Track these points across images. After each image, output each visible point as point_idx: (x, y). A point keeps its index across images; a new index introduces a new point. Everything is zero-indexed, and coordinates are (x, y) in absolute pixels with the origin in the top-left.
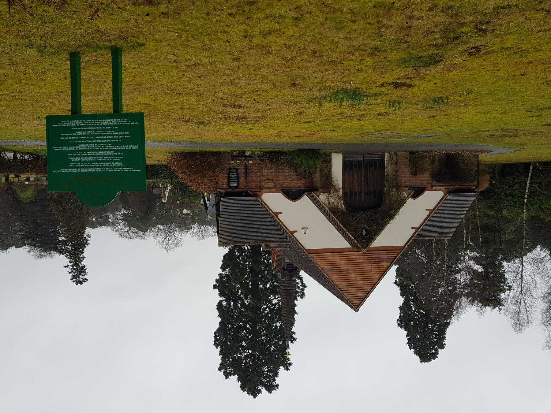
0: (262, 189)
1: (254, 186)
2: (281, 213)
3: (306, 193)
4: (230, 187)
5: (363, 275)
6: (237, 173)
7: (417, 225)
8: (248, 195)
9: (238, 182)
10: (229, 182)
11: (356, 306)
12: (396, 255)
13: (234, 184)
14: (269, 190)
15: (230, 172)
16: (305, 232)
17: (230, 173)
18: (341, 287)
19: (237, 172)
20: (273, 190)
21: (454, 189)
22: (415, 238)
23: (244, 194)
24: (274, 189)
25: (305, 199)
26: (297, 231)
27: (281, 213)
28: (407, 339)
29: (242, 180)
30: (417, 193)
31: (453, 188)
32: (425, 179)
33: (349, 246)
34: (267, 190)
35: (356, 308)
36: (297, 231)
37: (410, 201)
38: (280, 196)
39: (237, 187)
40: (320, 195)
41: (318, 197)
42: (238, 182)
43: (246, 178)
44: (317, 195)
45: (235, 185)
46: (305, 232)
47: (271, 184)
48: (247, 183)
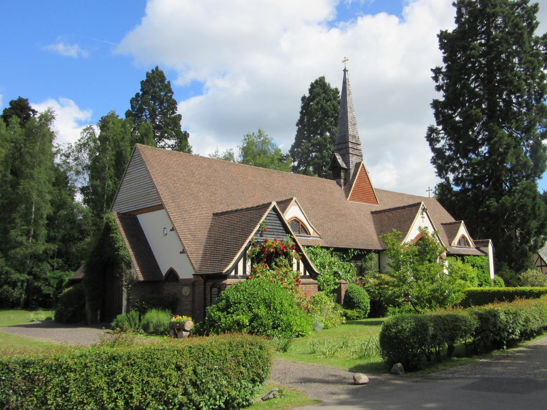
0: (192, 284)
1: (199, 288)
3: (163, 279)
8: (202, 276)
42: (211, 294)
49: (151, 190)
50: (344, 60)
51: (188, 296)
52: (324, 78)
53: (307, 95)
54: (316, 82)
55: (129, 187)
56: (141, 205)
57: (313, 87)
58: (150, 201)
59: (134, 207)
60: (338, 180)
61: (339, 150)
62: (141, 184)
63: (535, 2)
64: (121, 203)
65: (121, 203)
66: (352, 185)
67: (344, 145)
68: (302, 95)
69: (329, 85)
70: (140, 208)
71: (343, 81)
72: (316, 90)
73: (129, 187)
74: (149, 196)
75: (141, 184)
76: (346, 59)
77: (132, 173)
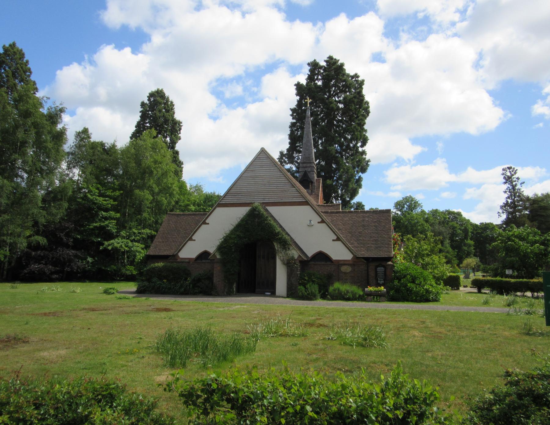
2: (333, 240)
4: (384, 266)
6: (377, 280)
7: (204, 226)
9: (376, 272)
10: (385, 271)
11: (263, 152)
12: (224, 198)
13: (380, 269)
14: (345, 262)
15: (384, 281)
17: (384, 280)
18: (276, 170)
19: (377, 281)
20: (342, 262)
23: (371, 260)
24: (340, 264)
25: (310, 254)
26: (319, 223)
27: (333, 240)
29: (372, 274)
30: (204, 255)
34: (347, 263)
35: (263, 151)
36: (319, 223)
37: (212, 249)
38: (334, 257)
39: (377, 267)
40: (298, 257)
41: (299, 255)
43: (368, 275)
44: (301, 257)
45: (379, 269)
47: (344, 269)
48: (368, 270)
51: (348, 273)
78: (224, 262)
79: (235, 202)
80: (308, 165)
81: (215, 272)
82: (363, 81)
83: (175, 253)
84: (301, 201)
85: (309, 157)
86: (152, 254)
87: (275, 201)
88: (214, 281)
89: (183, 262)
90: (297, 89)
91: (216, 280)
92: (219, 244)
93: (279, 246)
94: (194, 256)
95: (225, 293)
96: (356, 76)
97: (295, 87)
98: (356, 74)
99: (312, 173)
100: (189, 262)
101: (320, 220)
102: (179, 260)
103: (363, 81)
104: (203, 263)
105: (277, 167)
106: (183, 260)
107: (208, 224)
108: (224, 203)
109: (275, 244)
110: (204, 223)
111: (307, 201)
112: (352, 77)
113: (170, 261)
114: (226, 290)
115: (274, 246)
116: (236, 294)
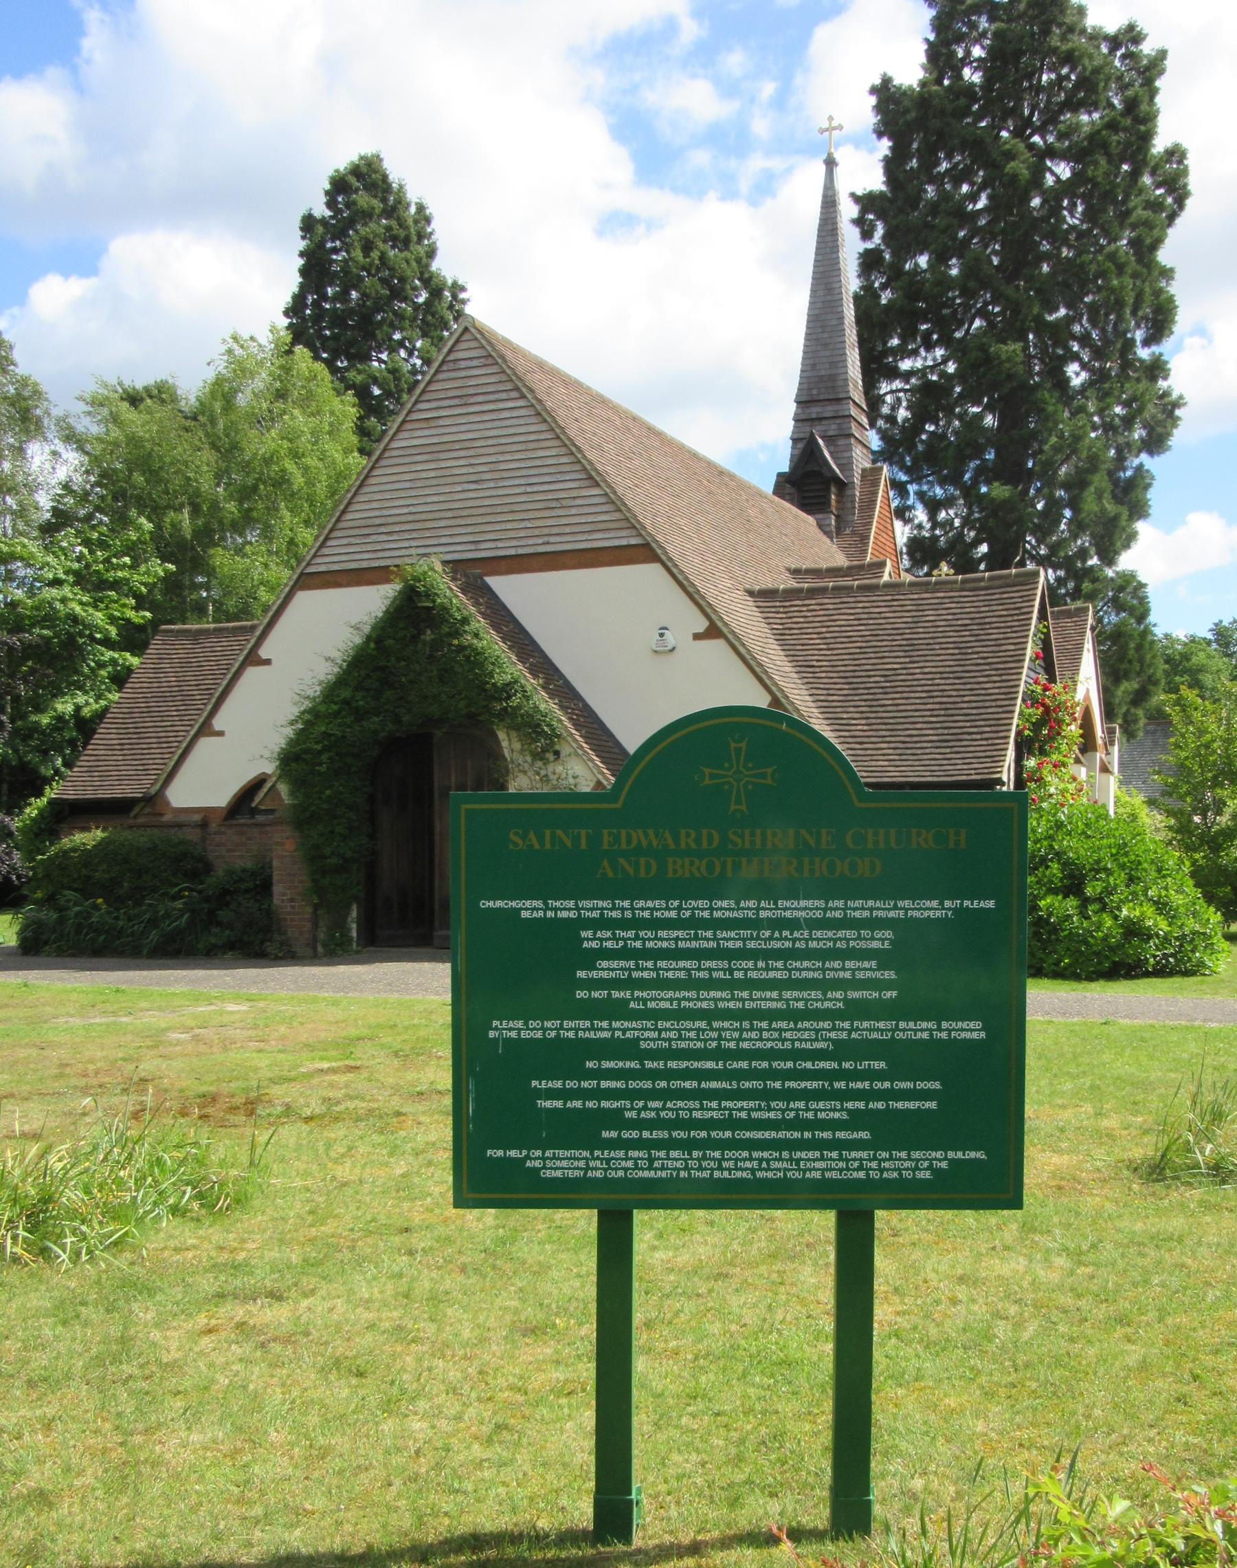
5: (443, 464)
16: (662, 635)
21: (132, 815)
22: (253, 628)
26: (697, 637)
28: (431, 234)
31: (136, 817)
32: (229, 851)
33: (495, 582)
36: (697, 637)
46: (662, 635)
49: (575, 494)
50: (826, 125)
52: (378, 158)
53: (321, 210)
54: (356, 171)
55: (432, 474)
56: (514, 543)
57: (339, 186)
58: (567, 530)
59: (472, 547)
60: (820, 516)
61: (812, 420)
62: (503, 466)
63: (1158, 46)
64: (383, 529)
65: (383, 529)
66: (868, 537)
67: (829, 408)
68: (303, 211)
69: (401, 186)
70: (512, 552)
71: (825, 196)
72: (363, 199)
73: (432, 474)
74: (562, 512)
75: (503, 466)
76: (834, 124)
77: (441, 422)
78: (303, 819)
79: (365, 565)
80: (829, 410)
81: (275, 863)
82: (1162, 54)
83: (153, 791)
84: (624, 542)
85: (832, 378)
86: (71, 795)
87: (521, 551)
88: (276, 901)
89: (180, 826)
90: (878, 108)
91: (281, 892)
92: (282, 743)
93: (517, 746)
94: (221, 798)
95: (320, 949)
96: (1132, 35)
97: (873, 100)
98: (1131, 27)
99: (842, 442)
100: (204, 825)
101: (701, 625)
102: (168, 818)
103: (1162, 54)
104: (256, 825)
105: (523, 397)
106: (182, 818)
107: (267, 662)
108: (322, 568)
109: (501, 735)
110: (253, 659)
111: (647, 546)
112: (1115, 42)
113: (141, 820)
114: (322, 936)
115: (498, 742)
116: (358, 952)
